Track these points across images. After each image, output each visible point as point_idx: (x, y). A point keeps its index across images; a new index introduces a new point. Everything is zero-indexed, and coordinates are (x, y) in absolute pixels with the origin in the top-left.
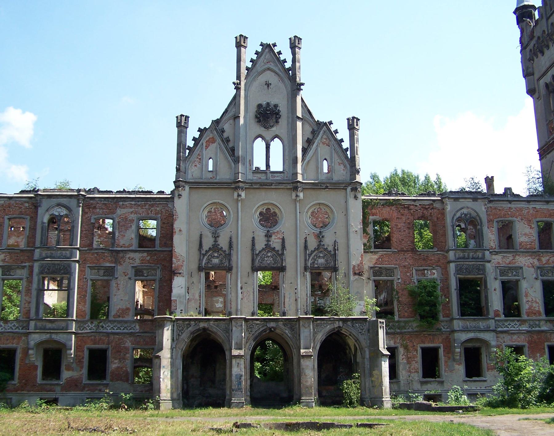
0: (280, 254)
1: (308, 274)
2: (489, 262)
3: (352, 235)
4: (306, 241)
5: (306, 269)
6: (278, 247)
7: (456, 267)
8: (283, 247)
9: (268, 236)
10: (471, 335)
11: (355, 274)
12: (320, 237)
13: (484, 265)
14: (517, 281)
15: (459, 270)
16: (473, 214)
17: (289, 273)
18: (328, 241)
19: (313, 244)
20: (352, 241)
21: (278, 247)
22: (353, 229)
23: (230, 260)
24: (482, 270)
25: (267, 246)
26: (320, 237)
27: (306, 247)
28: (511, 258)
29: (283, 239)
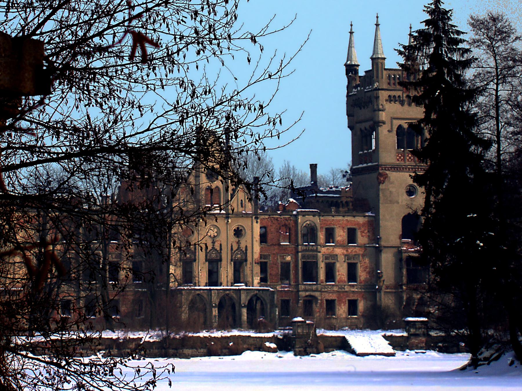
0: (220, 252)
1: (232, 263)
2: (320, 252)
3: (255, 242)
4: (232, 246)
5: (232, 260)
6: (218, 249)
7: (302, 255)
8: (221, 249)
9: (213, 242)
10: (307, 293)
11: (256, 263)
12: (238, 243)
13: (317, 254)
14: (334, 263)
15: (303, 257)
16: (313, 224)
17: (224, 262)
18: (243, 246)
19: (235, 247)
20: (255, 246)
21: (218, 249)
22: (254, 240)
23: (195, 256)
24: (316, 257)
25: (213, 248)
26: (238, 243)
27: (232, 249)
28: (332, 250)
29: (221, 245)
